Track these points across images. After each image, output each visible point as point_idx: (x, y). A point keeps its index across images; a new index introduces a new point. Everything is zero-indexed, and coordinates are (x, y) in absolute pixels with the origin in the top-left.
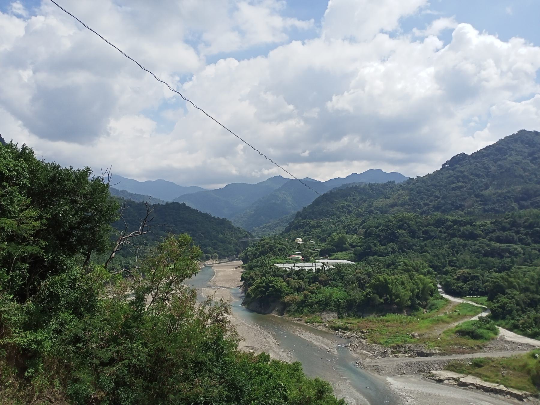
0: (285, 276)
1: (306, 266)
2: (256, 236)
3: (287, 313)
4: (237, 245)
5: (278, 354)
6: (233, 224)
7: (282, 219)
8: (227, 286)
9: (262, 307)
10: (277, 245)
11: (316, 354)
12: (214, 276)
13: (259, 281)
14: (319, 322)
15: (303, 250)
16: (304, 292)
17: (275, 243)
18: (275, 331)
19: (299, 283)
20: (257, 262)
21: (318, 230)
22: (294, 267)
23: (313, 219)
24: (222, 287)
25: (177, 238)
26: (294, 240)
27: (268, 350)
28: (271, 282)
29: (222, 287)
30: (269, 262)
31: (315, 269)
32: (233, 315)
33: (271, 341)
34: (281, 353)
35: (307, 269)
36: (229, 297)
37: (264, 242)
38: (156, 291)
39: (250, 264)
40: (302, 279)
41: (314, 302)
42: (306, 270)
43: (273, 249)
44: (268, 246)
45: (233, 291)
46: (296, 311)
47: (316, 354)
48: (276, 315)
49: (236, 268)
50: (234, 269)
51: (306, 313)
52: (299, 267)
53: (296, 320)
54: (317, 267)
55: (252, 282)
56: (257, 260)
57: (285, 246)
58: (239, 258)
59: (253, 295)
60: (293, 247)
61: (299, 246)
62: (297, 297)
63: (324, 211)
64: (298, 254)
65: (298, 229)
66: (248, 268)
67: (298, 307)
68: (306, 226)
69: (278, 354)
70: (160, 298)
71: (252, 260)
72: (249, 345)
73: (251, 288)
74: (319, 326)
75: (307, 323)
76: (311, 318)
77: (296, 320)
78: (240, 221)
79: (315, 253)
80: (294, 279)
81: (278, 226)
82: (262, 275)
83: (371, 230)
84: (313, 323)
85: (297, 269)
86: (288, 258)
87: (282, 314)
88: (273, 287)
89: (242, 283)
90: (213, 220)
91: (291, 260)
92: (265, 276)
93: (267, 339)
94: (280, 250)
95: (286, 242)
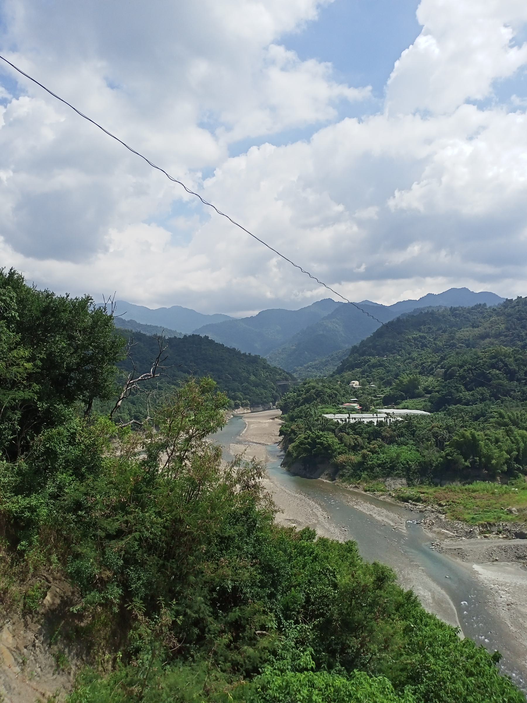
0: (336, 430)
1: (364, 418)
2: (299, 378)
3: (339, 478)
4: (274, 389)
5: (328, 530)
6: (268, 363)
7: (332, 355)
8: (262, 442)
9: (307, 470)
10: (326, 390)
11: (378, 532)
12: (246, 429)
13: (303, 436)
14: (382, 491)
15: (361, 396)
16: (363, 451)
17: (323, 388)
18: (325, 501)
19: (356, 439)
20: (300, 412)
21: (381, 370)
22: (349, 418)
23: (373, 356)
24: (256, 443)
25: (198, 382)
26: (349, 383)
27: (315, 525)
28: (318, 437)
29: (256, 443)
30: (315, 412)
31: (377, 421)
32: (270, 479)
33: (319, 514)
34: (332, 529)
35: (366, 421)
36: (264, 456)
37: (309, 386)
38: (172, 448)
39: (291, 414)
40: (360, 434)
41: (376, 464)
42: (365, 423)
43: (321, 395)
44: (314, 391)
45: (269, 448)
46: (352, 476)
47: (378, 532)
48: (325, 481)
49: (273, 419)
50: (271, 420)
51: (364, 478)
52: (355, 418)
53: (351, 487)
54: (379, 419)
55: (294, 437)
56: (300, 409)
57: (337, 391)
58: (277, 406)
59: (295, 454)
60: (347, 393)
61: (355, 391)
62: (353, 457)
63: (389, 345)
64: (354, 402)
65: (353, 369)
66: (288, 419)
67: (354, 470)
68: (364, 365)
69: (328, 530)
70: (177, 456)
71: (293, 409)
72: (291, 518)
73: (293, 444)
74: (382, 495)
75: (366, 491)
76: (371, 485)
77: (351, 487)
78: (277, 359)
79: (377, 400)
80: (348, 434)
81: (327, 365)
82: (307, 428)
83: (453, 370)
84: (374, 491)
85: (352, 421)
86: (341, 406)
87: (333, 479)
88: (321, 444)
89: (281, 438)
90: (242, 357)
91: (344, 410)
92: (311, 430)
93: (314, 510)
94: (329, 396)
95: (338, 386)
